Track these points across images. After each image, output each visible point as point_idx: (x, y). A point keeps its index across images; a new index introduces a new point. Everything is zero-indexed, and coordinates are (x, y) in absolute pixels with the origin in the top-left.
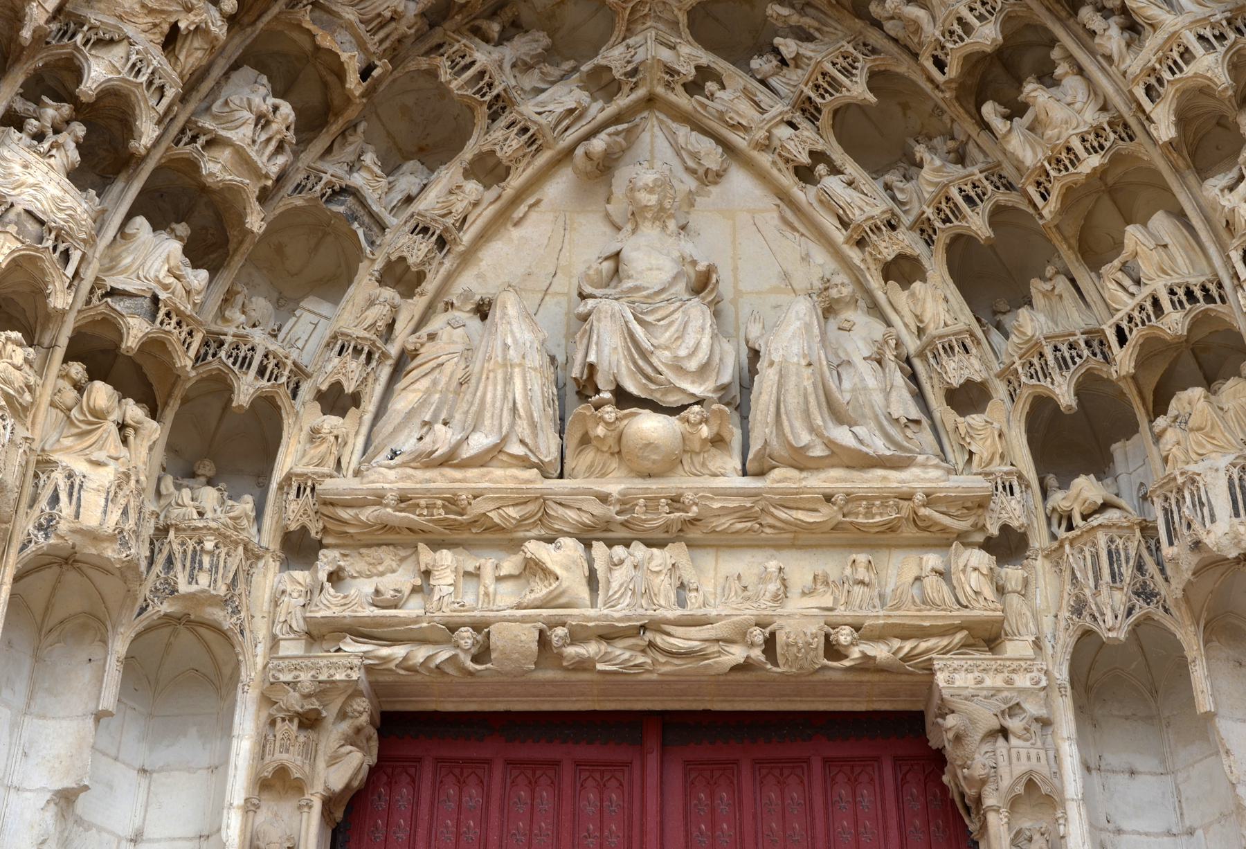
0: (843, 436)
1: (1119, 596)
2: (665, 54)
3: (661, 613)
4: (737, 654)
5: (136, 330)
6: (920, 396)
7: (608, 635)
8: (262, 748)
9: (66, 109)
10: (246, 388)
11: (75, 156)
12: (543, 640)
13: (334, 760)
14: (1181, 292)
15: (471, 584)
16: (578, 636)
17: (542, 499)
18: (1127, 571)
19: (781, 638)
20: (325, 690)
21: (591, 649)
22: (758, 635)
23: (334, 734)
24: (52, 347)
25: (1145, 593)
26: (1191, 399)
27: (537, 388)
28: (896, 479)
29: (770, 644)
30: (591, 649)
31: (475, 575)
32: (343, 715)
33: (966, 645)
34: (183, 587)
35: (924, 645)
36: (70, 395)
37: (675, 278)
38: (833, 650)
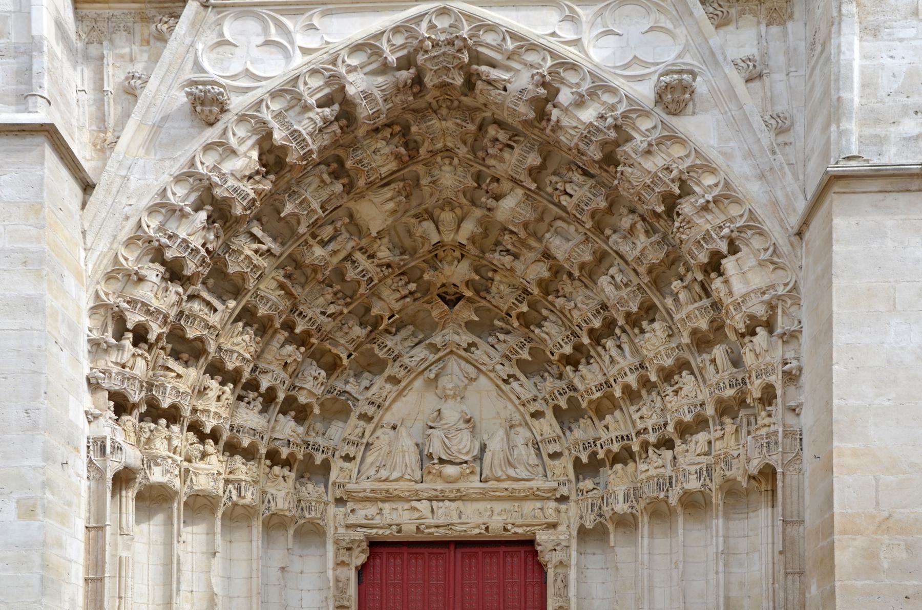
1: (592, 517)
2: (456, 338)
3: (454, 521)
4: (477, 531)
7: (437, 527)
8: (336, 556)
9: (256, 394)
11: (260, 407)
12: (418, 528)
13: (357, 557)
14: (620, 437)
15: (395, 511)
16: (428, 527)
18: (596, 509)
19: (490, 528)
20: (353, 541)
21: (432, 530)
22: (483, 527)
23: (356, 551)
24: (260, 459)
25: (600, 515)
26: (618, 466)
27: (413, 458)
29: (487, 529)
30: (432, 530)
31: (396, 509)
32: (359, 546)
33: (546, 527)
34: (307, 516)
35: (533, 528)
36: (268, 470)
37: (459, 419)
38: (505, 529)
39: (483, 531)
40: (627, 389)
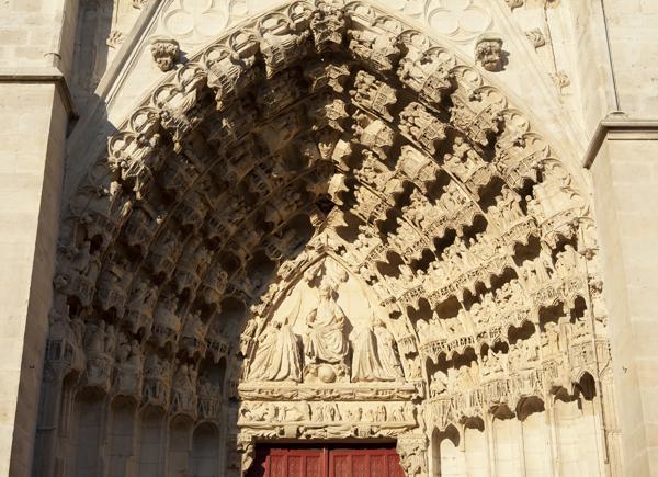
0: (377, 372)
4: (348, 434)
5: (192, 350)
6: (398, 357)
10: (218, 356)
16: (306, 429)
17: (297, 390)
18: (447, 411)
22: (353, 429)
24: (172, 357)
28: (389, 385)
29: (356, 431)
30: (310, 432)
34: (206, 416)
35: (396, 430)
38: (372, 433)
39: (353, 434)
40: (467, 293)
